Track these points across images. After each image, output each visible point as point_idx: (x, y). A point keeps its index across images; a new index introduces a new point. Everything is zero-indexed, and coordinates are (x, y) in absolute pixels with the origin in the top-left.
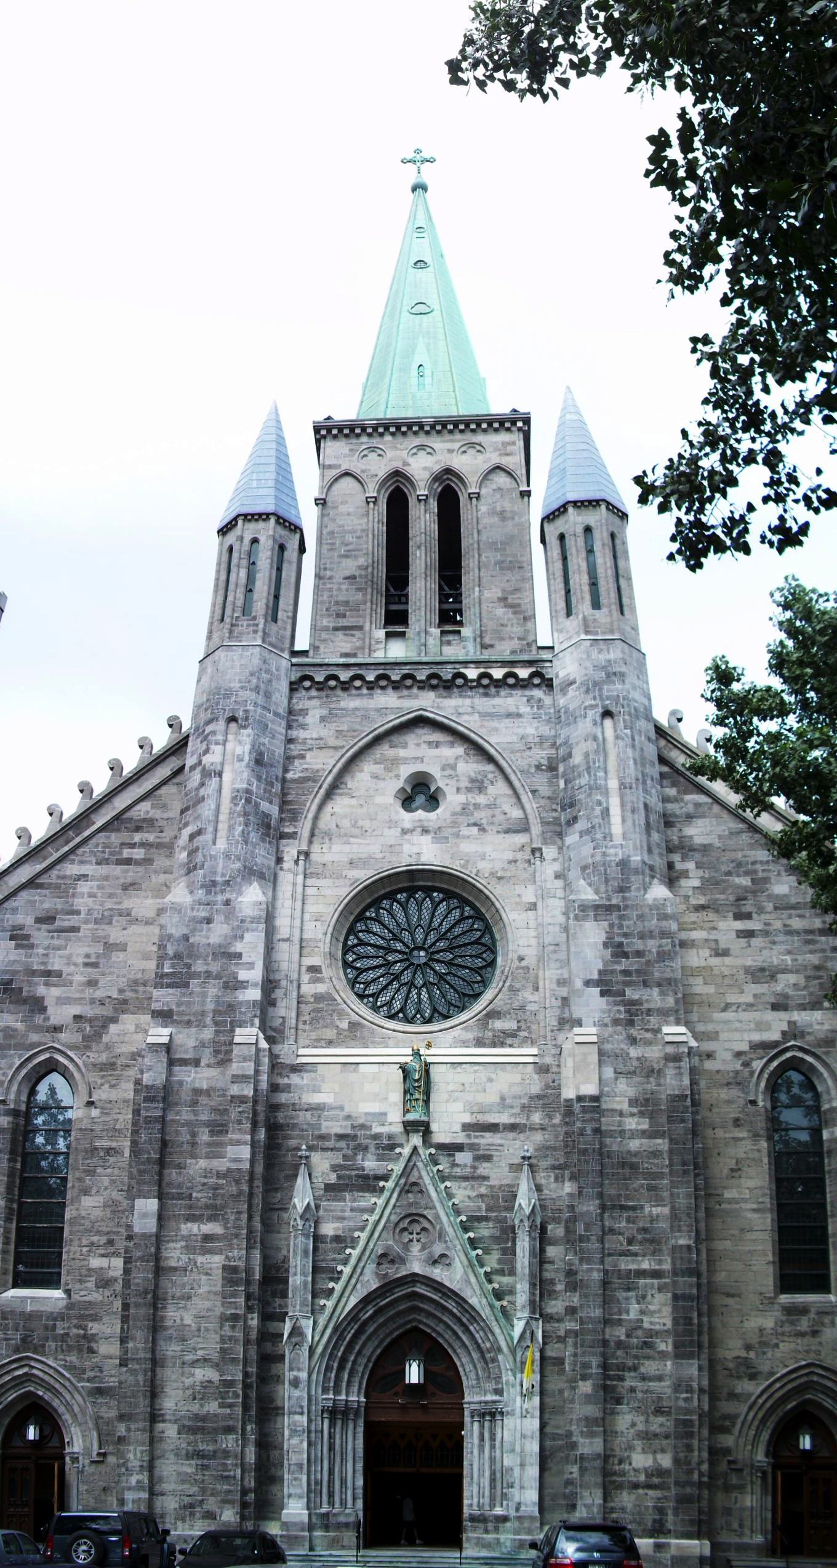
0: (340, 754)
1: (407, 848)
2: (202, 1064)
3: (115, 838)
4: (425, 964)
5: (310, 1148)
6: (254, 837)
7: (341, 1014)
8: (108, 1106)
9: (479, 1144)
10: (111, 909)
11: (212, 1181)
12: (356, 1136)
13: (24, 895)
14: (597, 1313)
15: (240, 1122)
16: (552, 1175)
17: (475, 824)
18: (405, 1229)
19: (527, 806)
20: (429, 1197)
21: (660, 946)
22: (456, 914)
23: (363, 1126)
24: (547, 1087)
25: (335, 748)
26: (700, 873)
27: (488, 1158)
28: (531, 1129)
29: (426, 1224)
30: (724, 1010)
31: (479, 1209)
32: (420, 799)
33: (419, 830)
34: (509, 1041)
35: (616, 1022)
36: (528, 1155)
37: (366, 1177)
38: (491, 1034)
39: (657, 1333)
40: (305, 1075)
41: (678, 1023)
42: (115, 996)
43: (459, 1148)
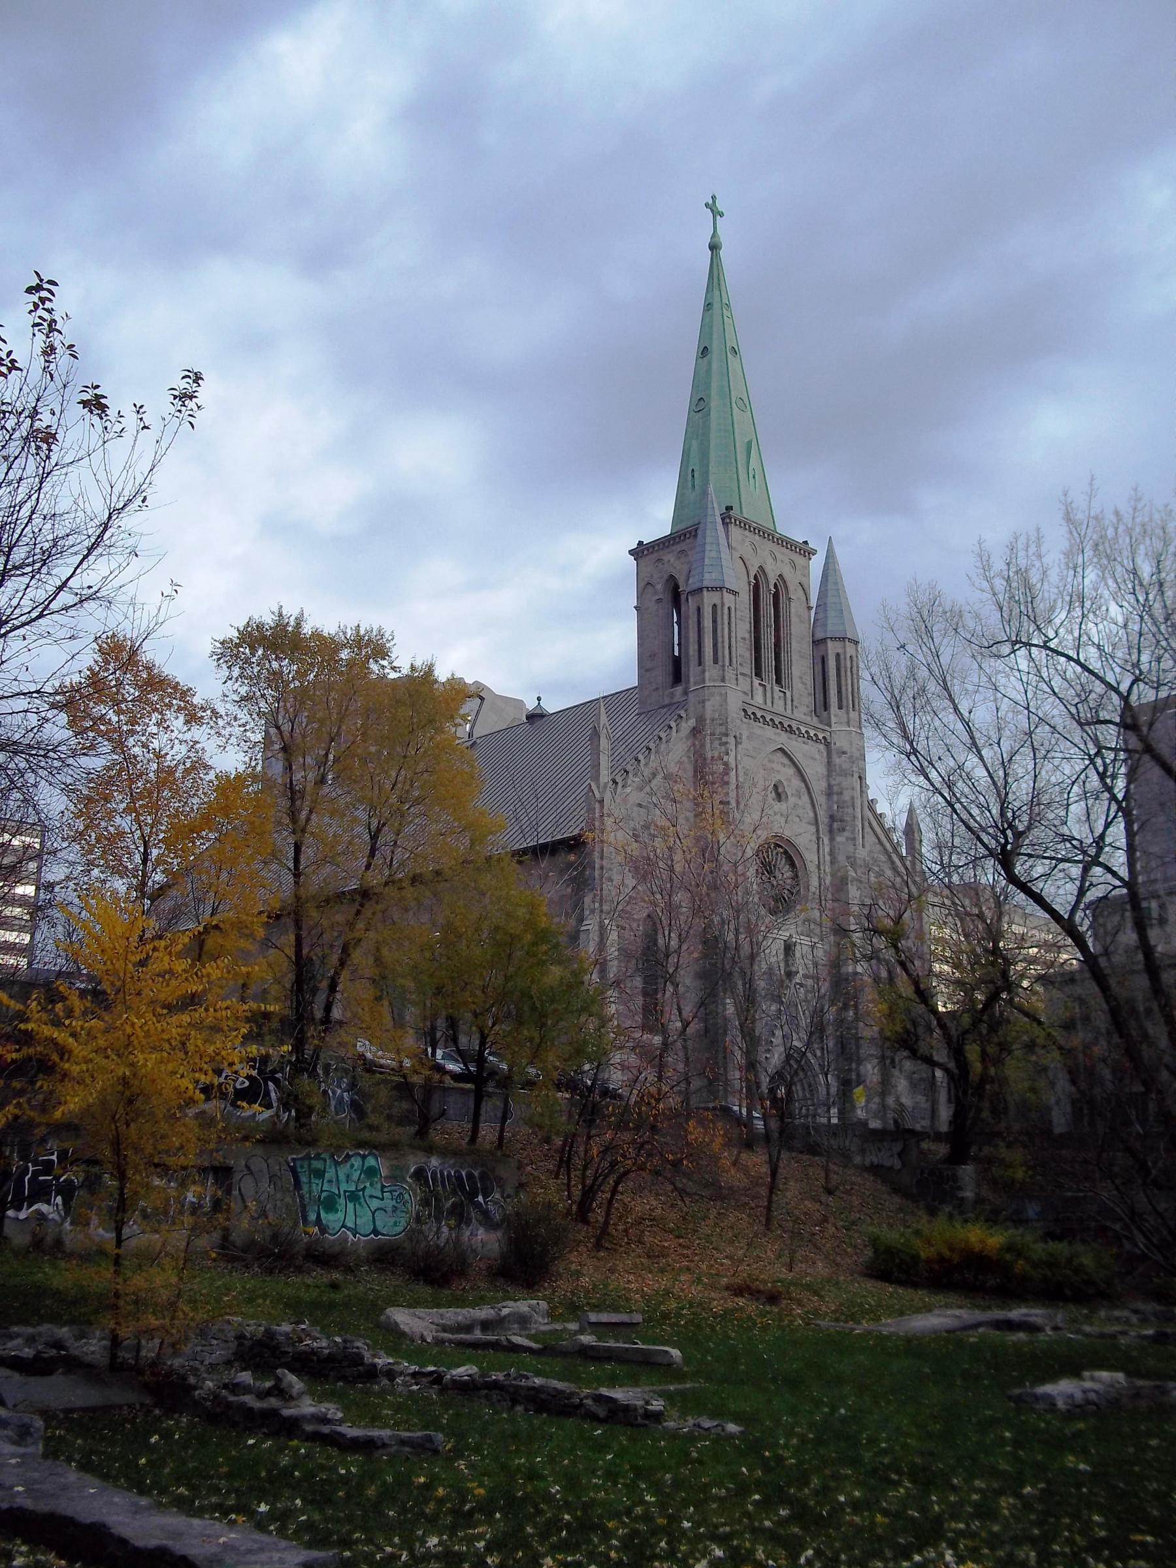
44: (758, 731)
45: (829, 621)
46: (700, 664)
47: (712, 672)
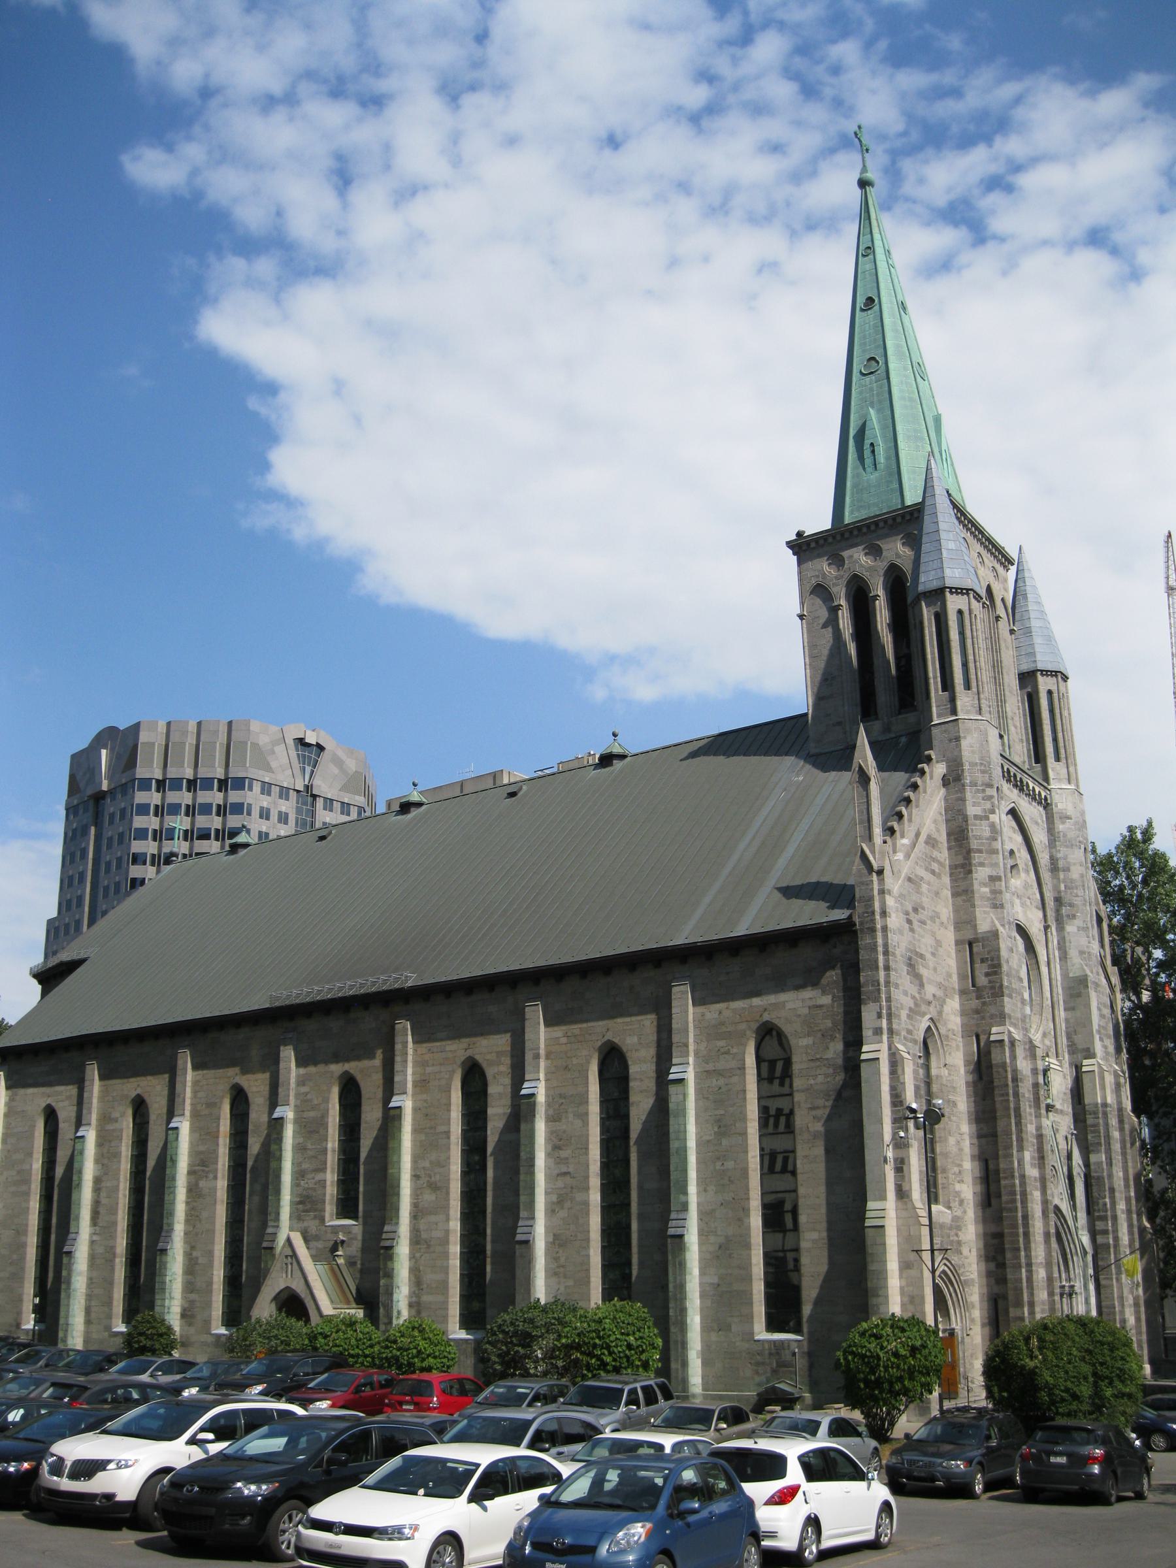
45: (1038, 649)
46: (944, 689)
47: (964, 700)
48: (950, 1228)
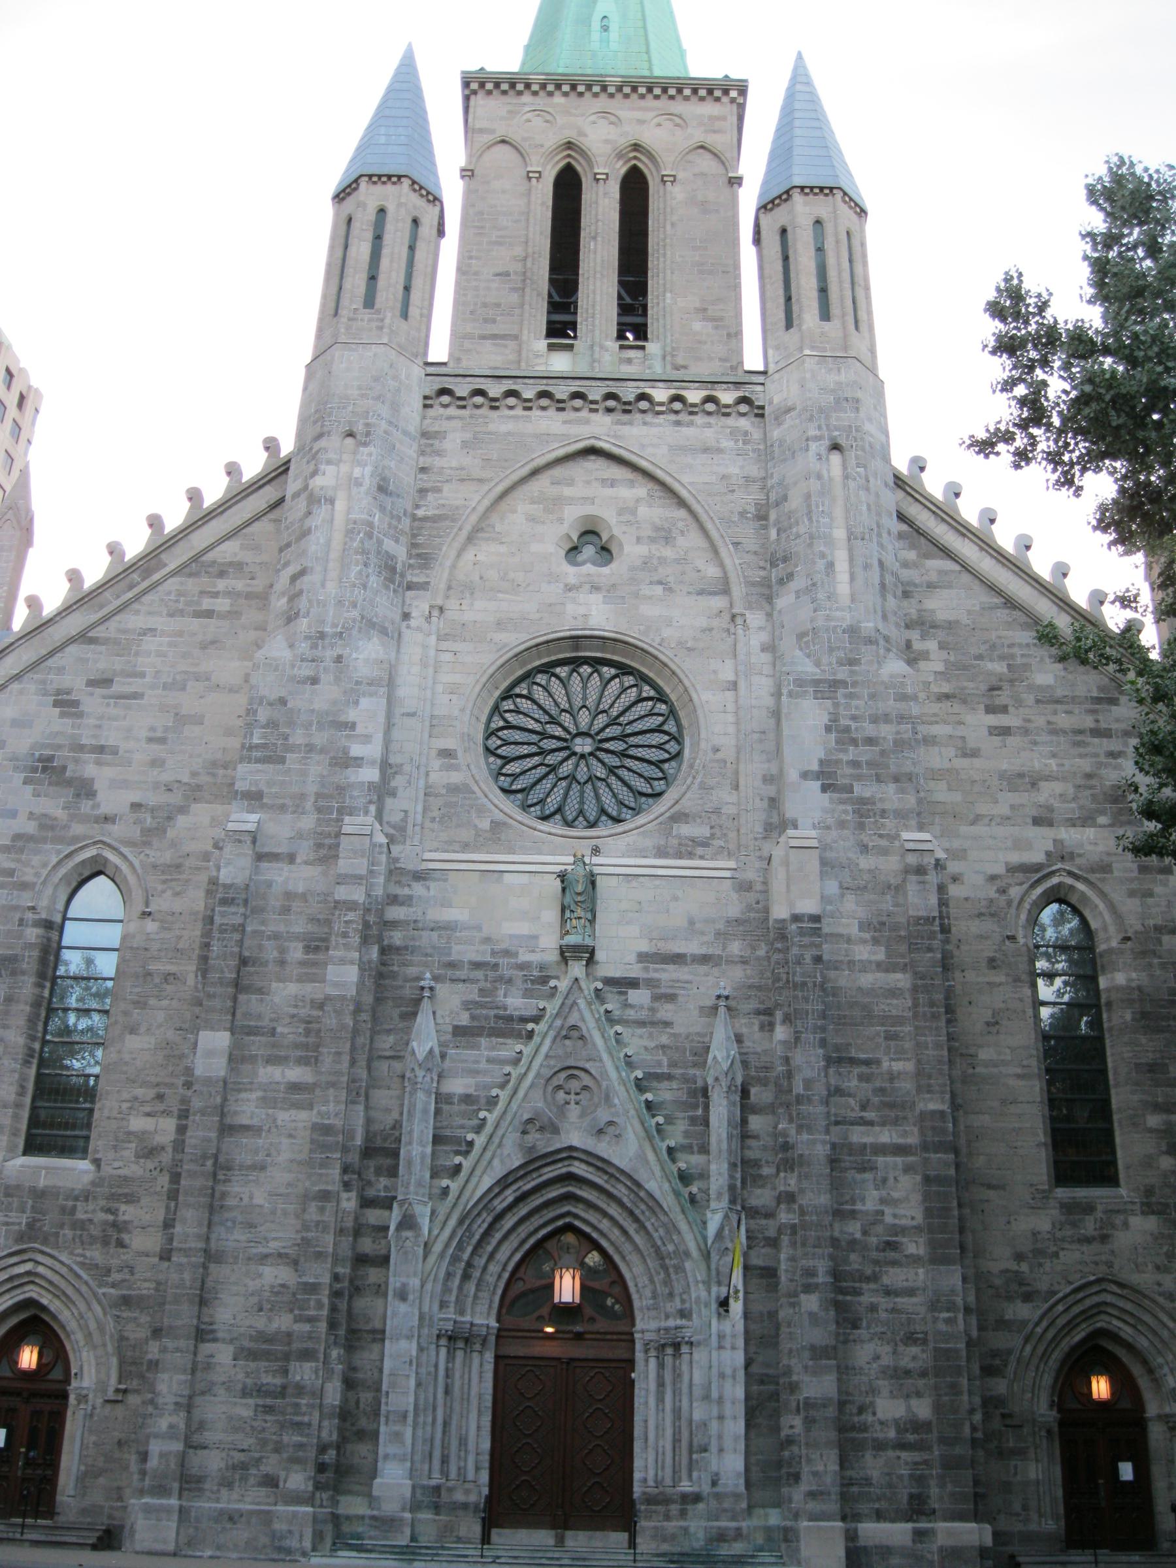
0: (486, 488)
1: (570, 608)
2: (298, 860)
3: (192, 585)
4: (591, 754)
5: (436, 978)
6: (374, 581)
7: (481, 811)
8: (170, 918)
9: (659, 980)
10: (186, 672)
11: (304, 1012)
12: (496, 965)
13: (72, 649)
14: (824, 1200)
15: (345, 935)
16: (756, 1022)
17: (660, 583)
18: (559, 1087)
19: (728, 562)
20: (594, 1045)
21: (898, 733)
22: (633, 693)
23: (507, 953)
24: (749, 908)
25: (481, 481)
26: (944, 654)
27: (671, 998)
28: (728, 962)
29: (586, 1080)
30: (973, 823)
31: (659, 1064)
32: (589, 551)
33: (588, 586)
34: (700, 851)
35: (842, 824)
36: (726, 993)
37: (510, 1019)
38: (675, 842)
39: (903, 1230)
40: (432, 885)
41: (921, 828)
42: (186, 780)
43: (633, 983)
44: (504, 428)
48: (86, 1196)
